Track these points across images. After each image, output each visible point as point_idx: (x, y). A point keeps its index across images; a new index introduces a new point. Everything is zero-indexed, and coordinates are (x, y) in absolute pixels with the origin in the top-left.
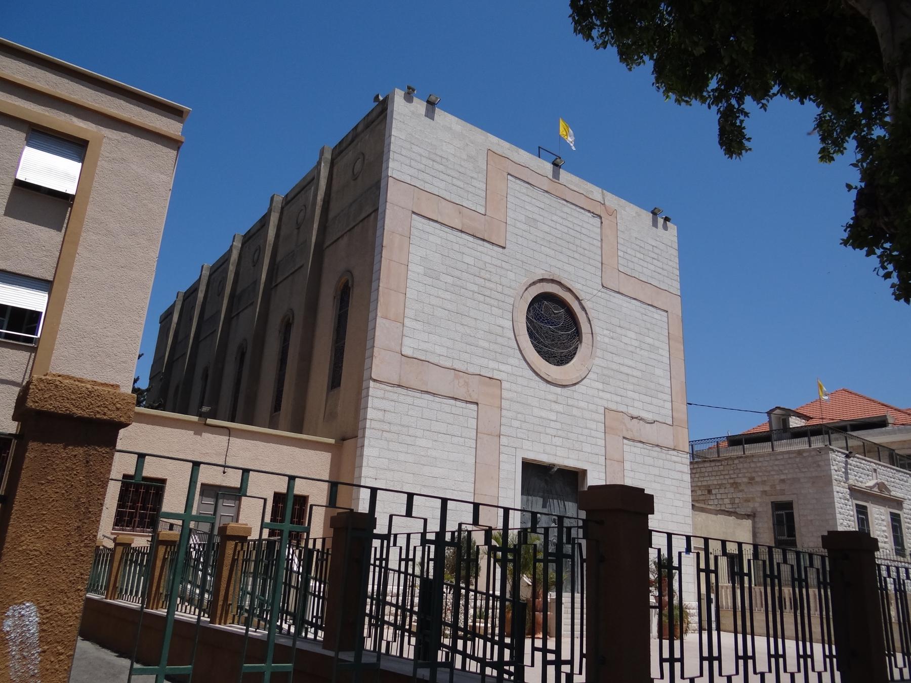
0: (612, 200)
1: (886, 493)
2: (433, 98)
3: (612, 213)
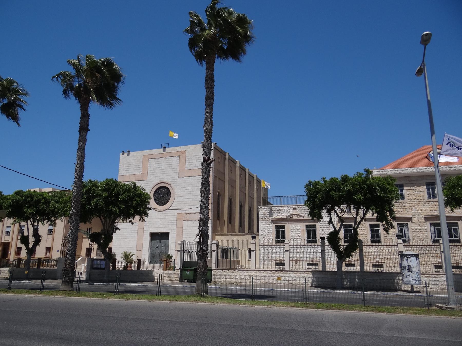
0: (184, 148)
1: (301, 217)
2: (128, 151)
3: (184, 153)
